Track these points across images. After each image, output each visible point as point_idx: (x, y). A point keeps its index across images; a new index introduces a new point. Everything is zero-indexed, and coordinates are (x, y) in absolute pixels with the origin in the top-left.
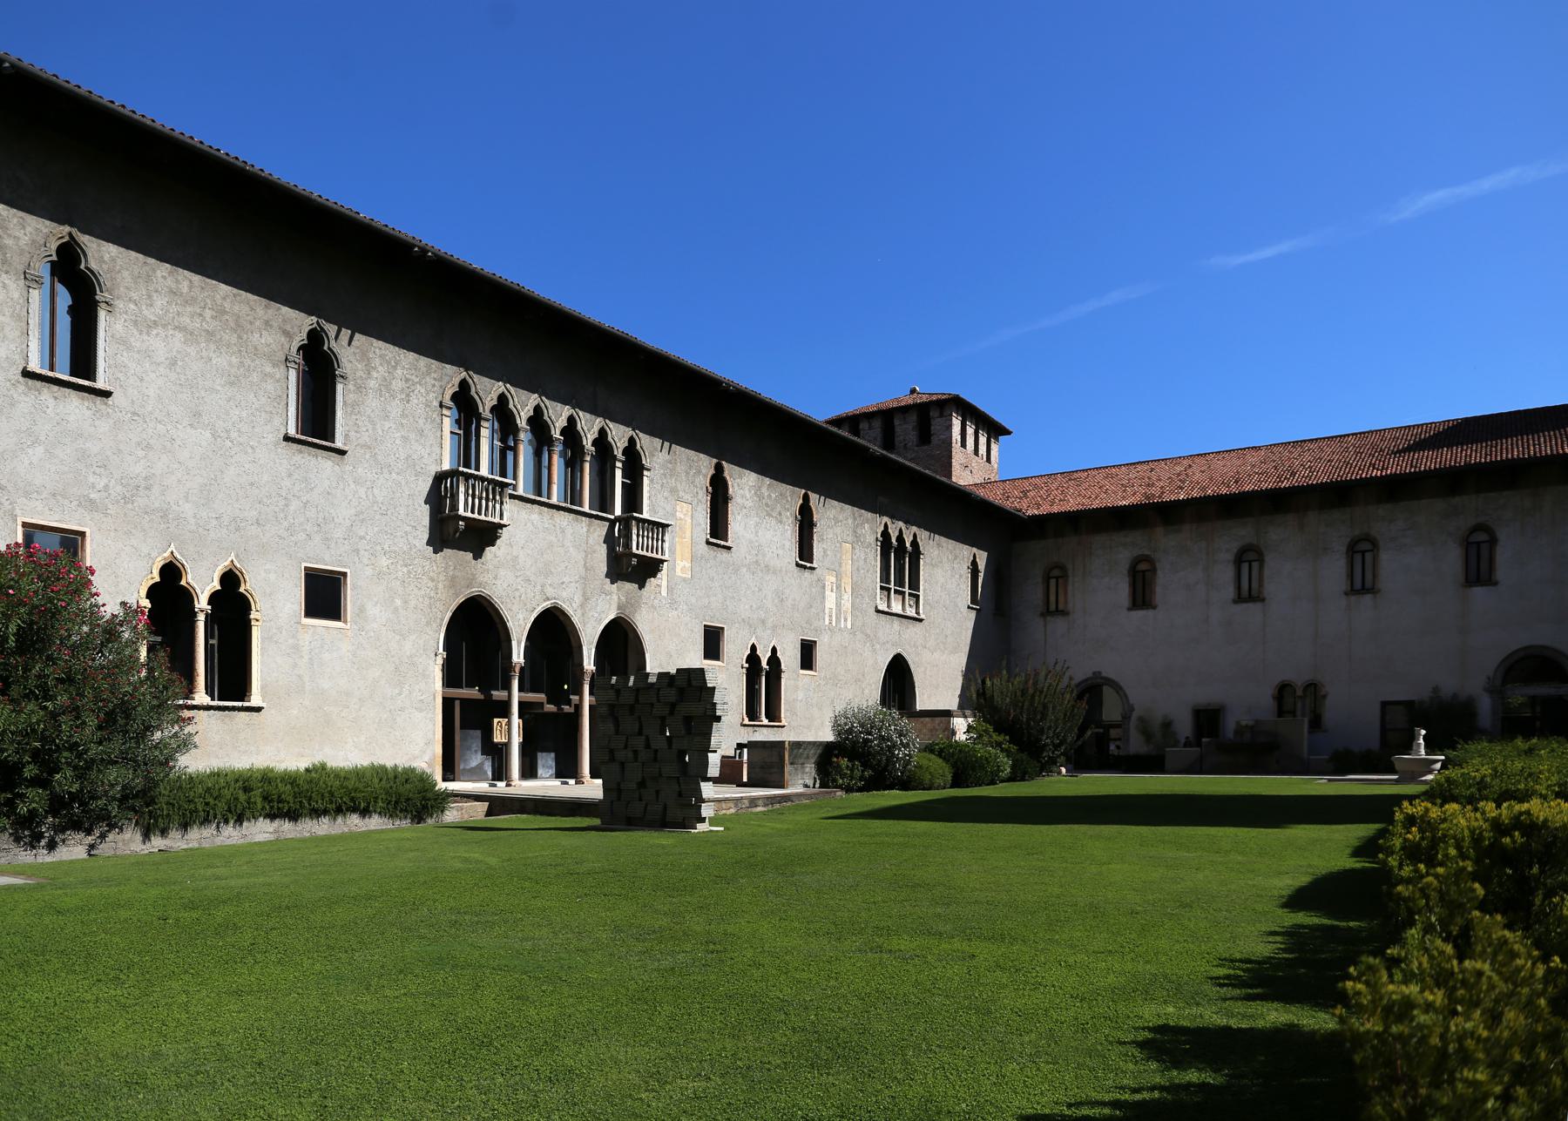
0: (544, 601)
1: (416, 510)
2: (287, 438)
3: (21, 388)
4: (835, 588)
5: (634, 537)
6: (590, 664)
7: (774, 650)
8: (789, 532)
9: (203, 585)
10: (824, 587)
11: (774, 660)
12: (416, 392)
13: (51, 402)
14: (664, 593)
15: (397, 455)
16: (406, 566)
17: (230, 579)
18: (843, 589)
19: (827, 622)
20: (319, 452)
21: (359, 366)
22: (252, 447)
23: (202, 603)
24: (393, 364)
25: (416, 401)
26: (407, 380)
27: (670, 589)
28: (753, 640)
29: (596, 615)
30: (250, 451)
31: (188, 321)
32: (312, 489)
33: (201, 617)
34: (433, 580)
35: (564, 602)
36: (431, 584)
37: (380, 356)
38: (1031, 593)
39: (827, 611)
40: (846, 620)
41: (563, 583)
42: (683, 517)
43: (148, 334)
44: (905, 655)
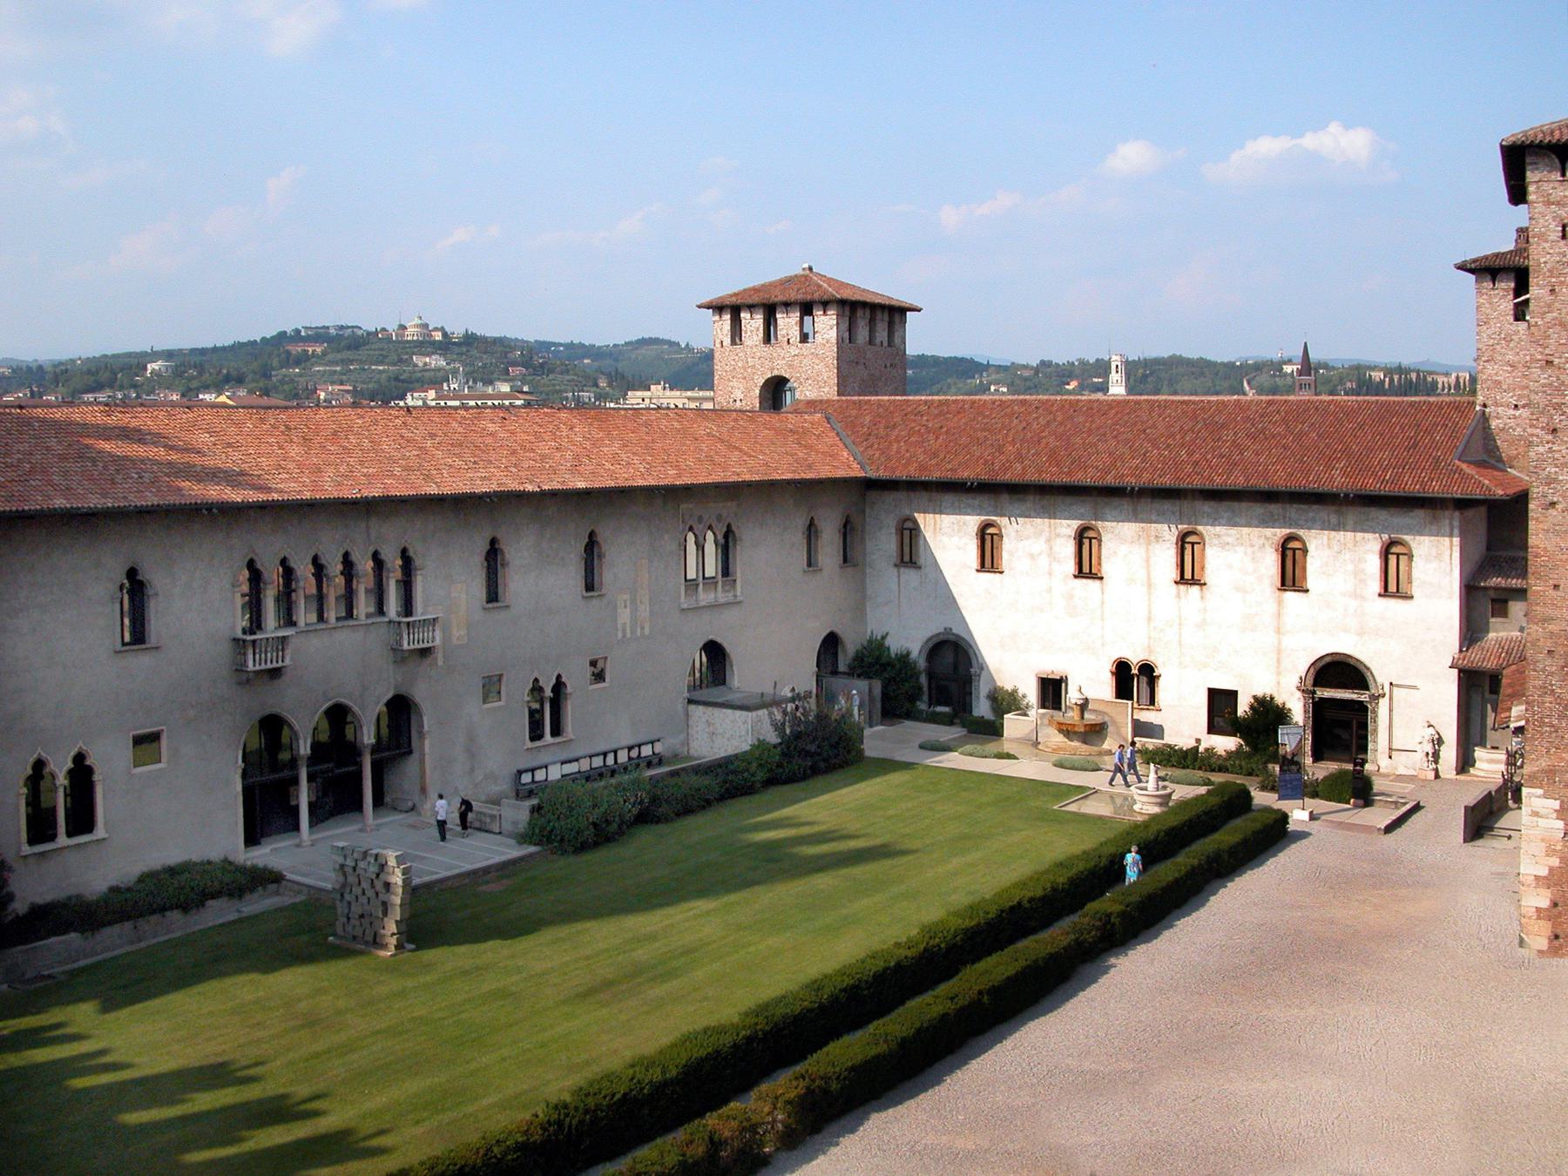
2: (116, 652)
4: (628, 604)
5: (405, 636)
6: (369, 738)
7: (559, 677)
9: (60, 768)
10: (615, 608)
11: (559, 686)
14: (440, 663)
17: (80, 758)
19: (620, 635)
23: (62, 780)
28: (536, 675)
33: (61, 790)
34: (231, 714)
38: (883, 544)
39: (619, 626)
40: (642, 628)
42: (456, 595)
44: (719, 640)
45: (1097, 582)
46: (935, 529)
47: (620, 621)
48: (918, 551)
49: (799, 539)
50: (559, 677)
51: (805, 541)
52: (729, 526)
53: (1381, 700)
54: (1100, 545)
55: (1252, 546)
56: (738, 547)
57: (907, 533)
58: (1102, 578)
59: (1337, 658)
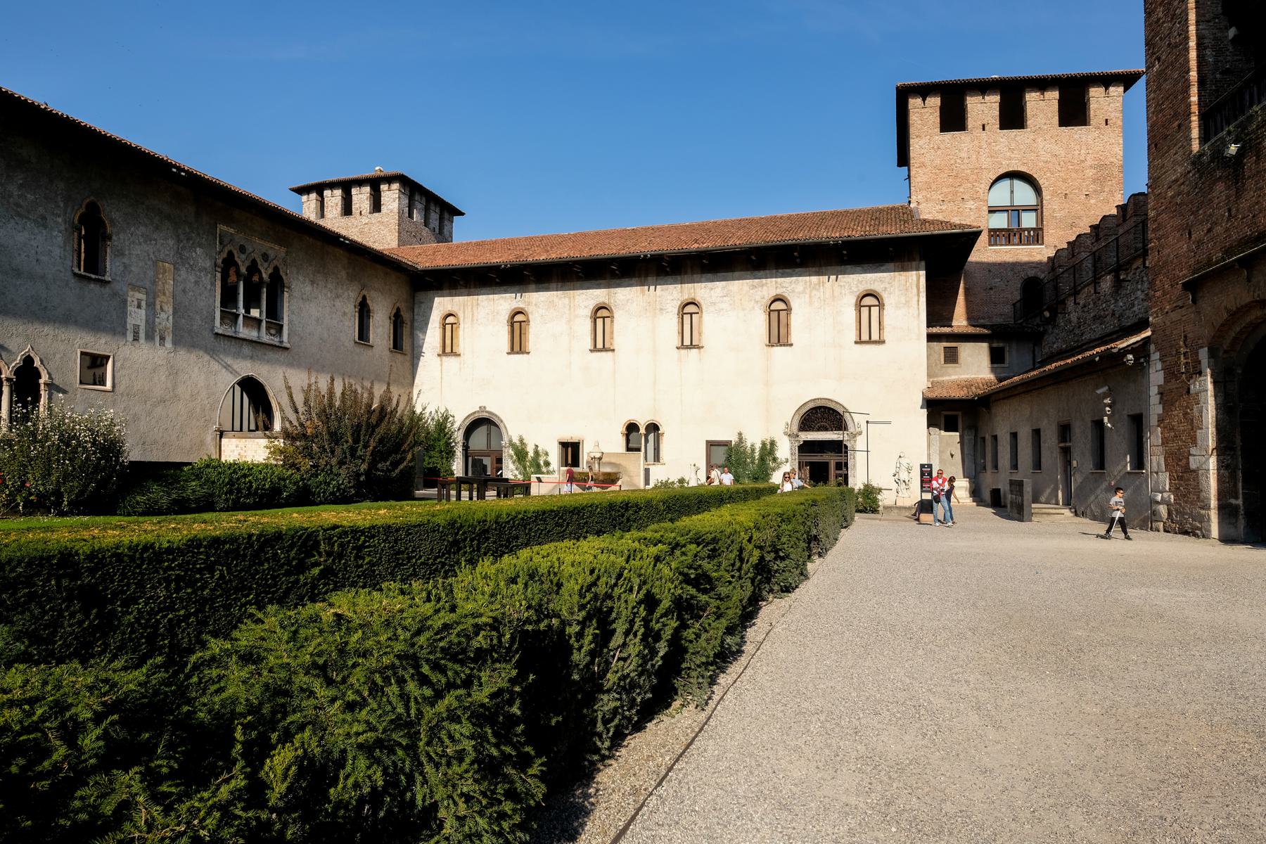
4: (143, 304)
8: (60, 239)
10: (125, 302)
18: (158, 307)
45: (610, 354)
46: (472, 320)
47: (131, 321)
48: (458, 338)
49: (351, 310)
50: (28, 360)
51: (357, 314)
52: (276, 269)
53: (858, 438)
54: (612, 321)
55: (743, 309)
56: (286, 295)
57: (448, 327)
58: (613, 350)
59: (819, 404)
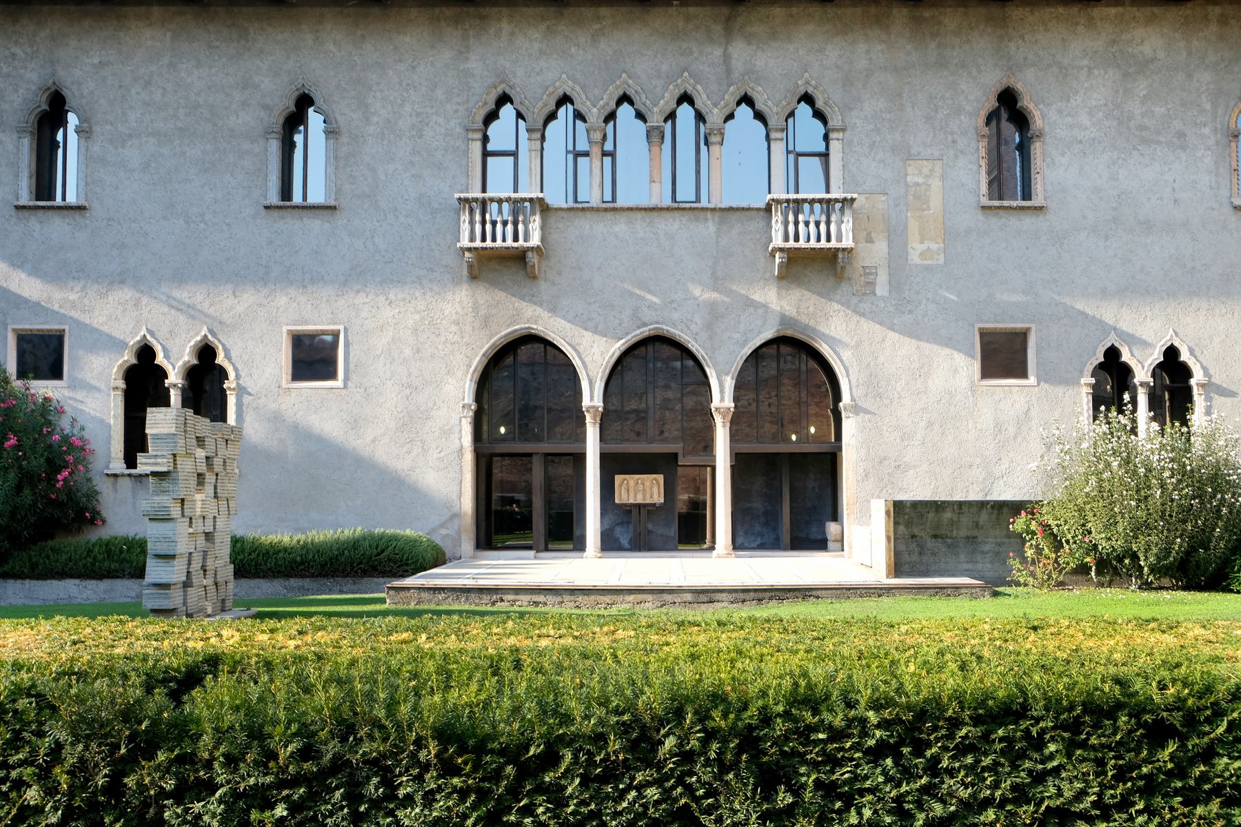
0: (639, 328)
1: (433, 250)
3: (13, 220)
12: (431, 124)
13: (37, 227)
14: (882, 289)
15: (406, 197)
16: (419, 312)
17: (206, 352)
20: (317, 212)
21: (355, 116)
22: (228, 225)
24: (400, 102)
25: (432, 134)
26: (418, 114)
27: (895, 285)
29: (737, 336)
30: (225, 228)
31: (162, 125)
32: (297, 252)
35: (674, 325)
36: (454, 328)
37: (382, 99)
41: (672, 302)
42: (921, 180)
43: (123, 147)
